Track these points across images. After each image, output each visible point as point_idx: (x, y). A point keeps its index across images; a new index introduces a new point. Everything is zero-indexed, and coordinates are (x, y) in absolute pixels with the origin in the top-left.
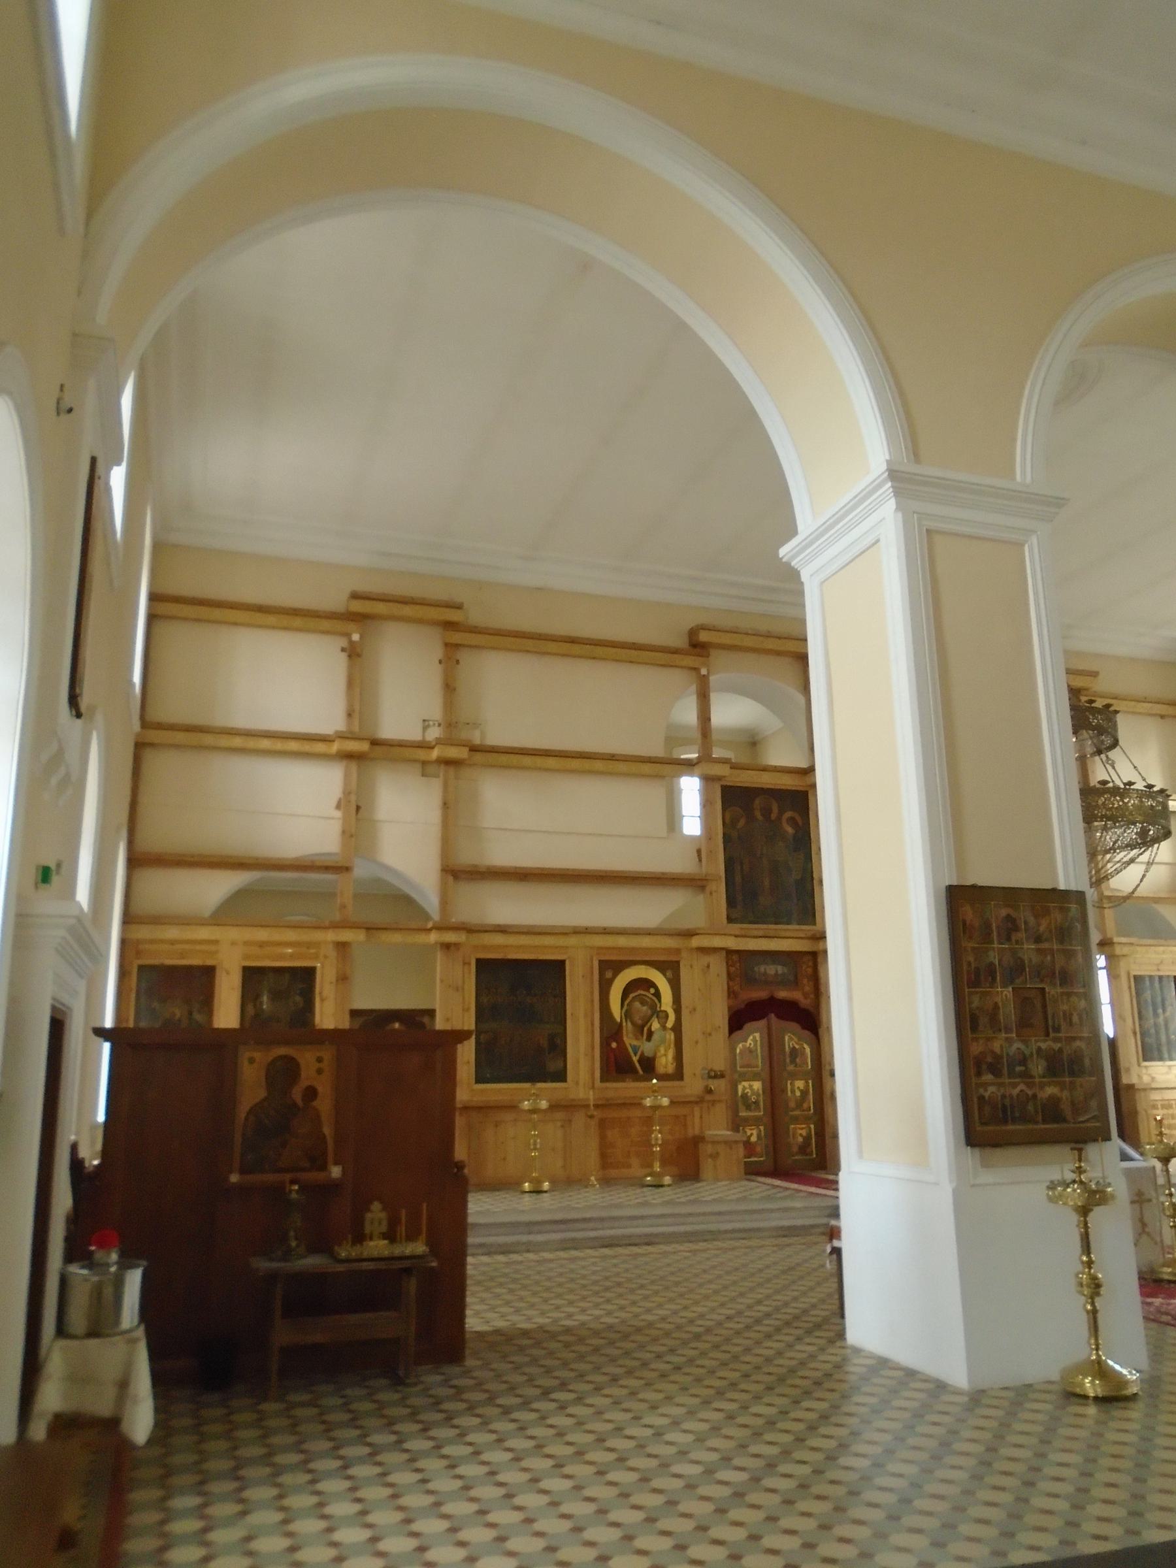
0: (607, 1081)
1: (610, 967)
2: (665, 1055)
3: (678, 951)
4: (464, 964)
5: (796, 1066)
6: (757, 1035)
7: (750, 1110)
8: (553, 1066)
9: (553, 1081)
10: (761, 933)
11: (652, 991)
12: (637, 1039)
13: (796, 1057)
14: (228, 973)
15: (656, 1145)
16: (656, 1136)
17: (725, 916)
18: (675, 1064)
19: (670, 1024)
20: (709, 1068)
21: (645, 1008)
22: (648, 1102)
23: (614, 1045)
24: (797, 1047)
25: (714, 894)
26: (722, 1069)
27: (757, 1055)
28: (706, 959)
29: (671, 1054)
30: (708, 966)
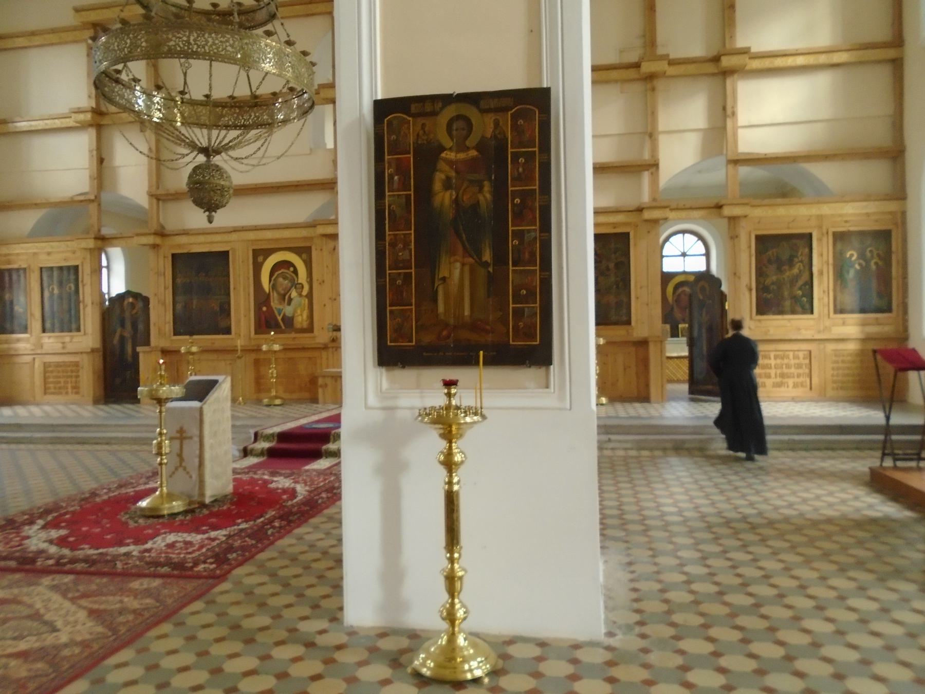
1: (260, 255)
2: (301, 315)
3: (310, 239)
4: (164, 257)
8: (223, 324)
9: (223, 334)
11: (292, 269)
12: (280, 303)
15: (272, 377)
18: (308, 322)
19: (305, 293)
20: (334, 324)
21: (286, 281)
22: (264, 348)
23: (264, 309)
29: (305, 314)
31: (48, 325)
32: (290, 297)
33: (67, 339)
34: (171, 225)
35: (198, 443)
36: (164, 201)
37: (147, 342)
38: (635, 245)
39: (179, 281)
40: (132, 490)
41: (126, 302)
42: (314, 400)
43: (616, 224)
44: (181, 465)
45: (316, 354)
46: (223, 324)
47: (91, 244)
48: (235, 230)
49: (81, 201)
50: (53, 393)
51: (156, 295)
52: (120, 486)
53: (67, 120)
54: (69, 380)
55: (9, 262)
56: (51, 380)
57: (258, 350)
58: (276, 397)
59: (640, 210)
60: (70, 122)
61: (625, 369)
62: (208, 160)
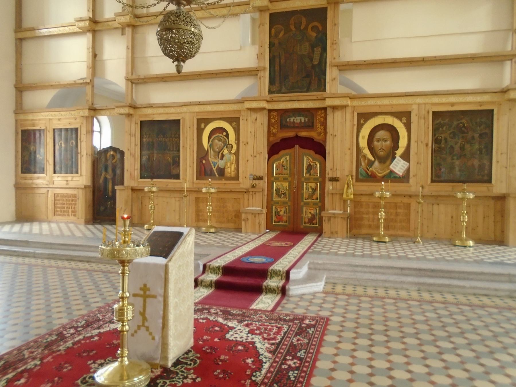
0: (200, 180)
3: (239, 111)
4: (135, 123)
5: (310, 175)
6: (288, 157)
7: (281, 198)
9: (174, 179)
10: (288, 99)
13: (311, 169)
14: (49, 132)
15: (209, 212)
16: (209, 208)
17: (267, 89)
19: (233, 151)
20: (254, 175)
22: (204, 190)
24: (312, 164)
25: (262, 78)
26: (262, 175)
27: (287, 167)
28: (254, 116)
30: (256, 120)
31: (58, 168)
32: (223, 153)
33: (69, 179)
34: (140, 101)
35: (162, 303)
36: (137, 84)
37: (122, 183)
38: (498, 119)
39: (145, 140)
40: (96, 332)
41: (108, 155)
42: (239, 230)
43: (483, 102)
44: (143, 325)
45: (240, 196)
46: (174, 172)
47: (86, 113)
48: (185, 105)
49: (81, 84)
50: (60, 215)
51: (129, 150)
52: (88, 324)
53: (73, 27)
54: (70, 206)
55: (34, 125)
56: (59, 206)
57: (199, 191)
58: (211, 227)
59: (505, 91)
60: (75, 29)
61: (484, 218)
62: (179, 9)
